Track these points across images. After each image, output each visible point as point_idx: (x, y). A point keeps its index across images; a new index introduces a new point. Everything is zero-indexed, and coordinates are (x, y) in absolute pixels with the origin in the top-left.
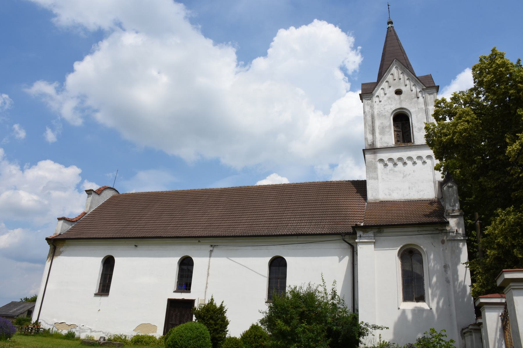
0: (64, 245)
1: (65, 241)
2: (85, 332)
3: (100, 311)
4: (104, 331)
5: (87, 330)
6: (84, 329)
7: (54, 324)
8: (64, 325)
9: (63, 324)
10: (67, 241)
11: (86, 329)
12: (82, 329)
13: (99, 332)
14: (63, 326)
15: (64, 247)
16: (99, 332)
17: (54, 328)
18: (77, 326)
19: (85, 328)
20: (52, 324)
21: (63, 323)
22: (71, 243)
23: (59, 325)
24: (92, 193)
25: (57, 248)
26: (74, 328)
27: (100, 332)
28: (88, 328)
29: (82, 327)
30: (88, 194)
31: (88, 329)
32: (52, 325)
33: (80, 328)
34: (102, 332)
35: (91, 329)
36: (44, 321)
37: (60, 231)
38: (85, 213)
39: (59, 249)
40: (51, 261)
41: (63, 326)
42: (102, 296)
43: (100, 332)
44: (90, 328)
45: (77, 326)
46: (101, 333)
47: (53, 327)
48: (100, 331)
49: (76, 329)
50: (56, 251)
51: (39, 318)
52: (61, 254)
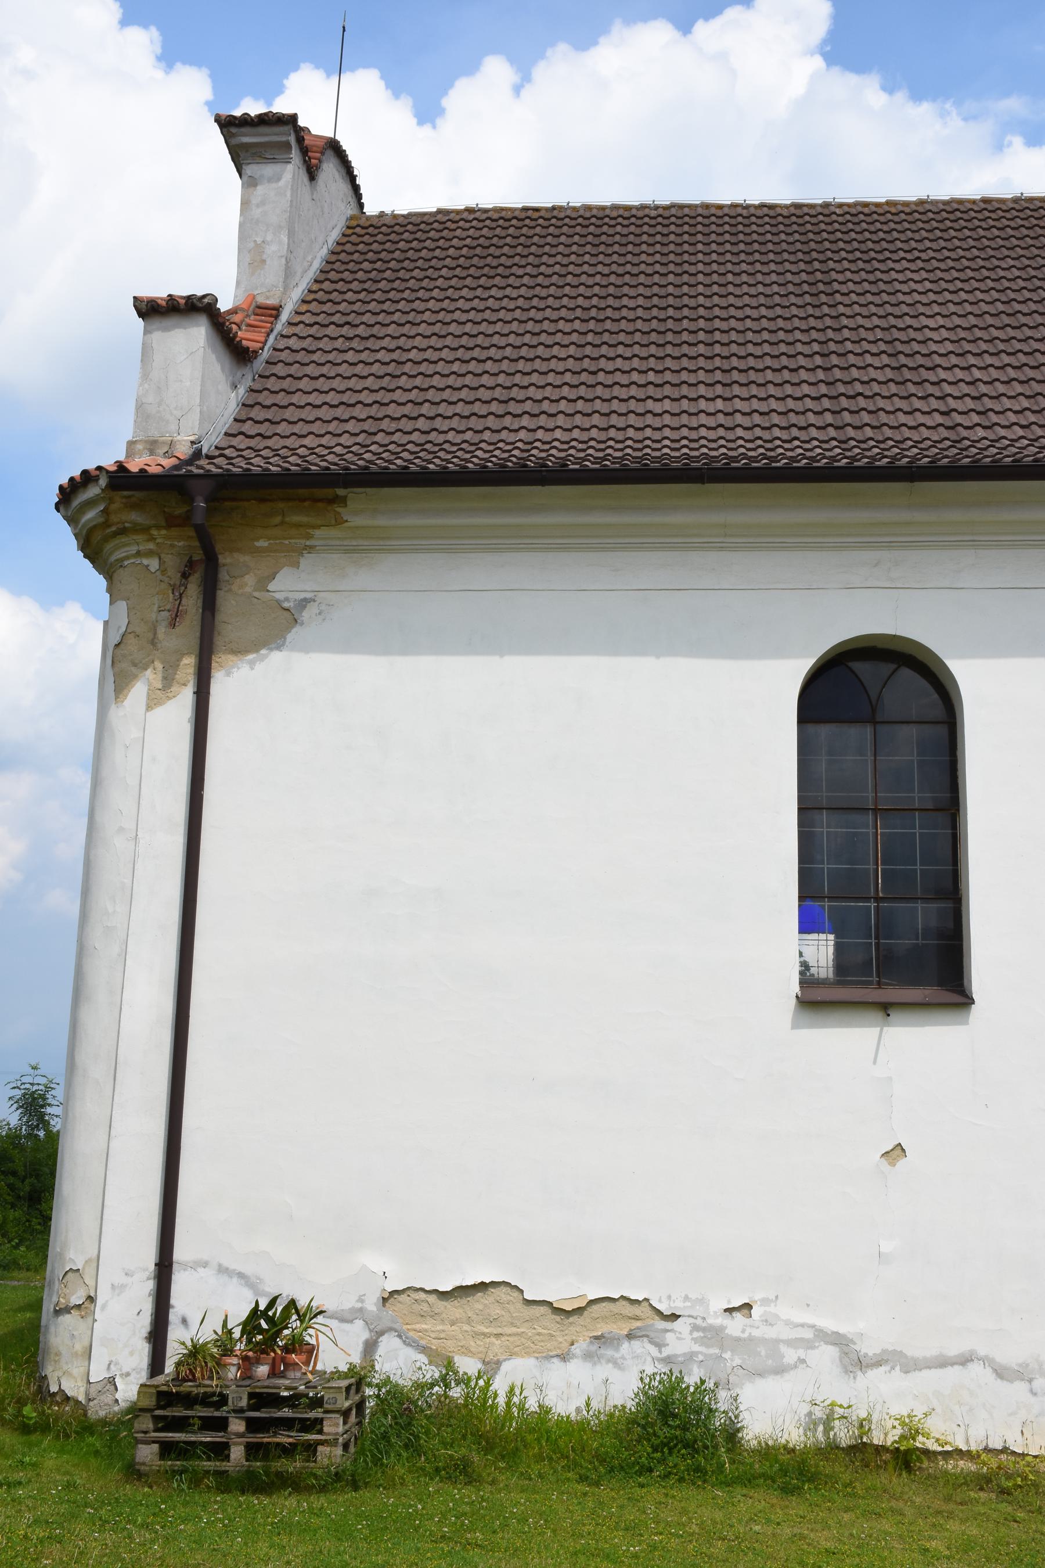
0: (311, 549)
1: (343, 501)
2: (780, 1370)
3: (902, 1163)
4: (1009, 1355)
5: (801, 1353)
6: (751, 1339)
7: (371, 1305)
8: (496, 1311)
9: (479, 1301)
10: (358, 498)
11: (792, 1343)
12: (738, 1339)
13: (943, 1363)
14: (493, 1321)
15: (307, 561)
16: (943, 1363)
17: (388, 1344)
18: (675, 1317)
19: (770, 1333)
20: (349, 1303)
21: (482, 1287)
22: (381, 521)
23: (434, 1315)
24: (287, 146)
25: (223, 575)
26: (630, 1336)
27: (965, 1360)
28: (809, 1334)
29: (735, 1326)
30: (240, 155)
31: (809, 1345)
32: (358, 1313)
33: (713, 1335)
34: (986, 1360)
35: (839, 1341)
36: (241, 1275)
37: (196, 416)
38: (259, 307)
39: (250, 580)
40: (186, 697)
41: (493, 1321)
42: (895, 1015)
43: (965, 1360)
44: (829, 1324)
45: (675, 1317)
46: (976, 1369)
47: (366, 1335)
48: (953, 1350)
49: (659, 1346)
50: (228, 603)
51: (180, 1253)
52: (295, 635)
